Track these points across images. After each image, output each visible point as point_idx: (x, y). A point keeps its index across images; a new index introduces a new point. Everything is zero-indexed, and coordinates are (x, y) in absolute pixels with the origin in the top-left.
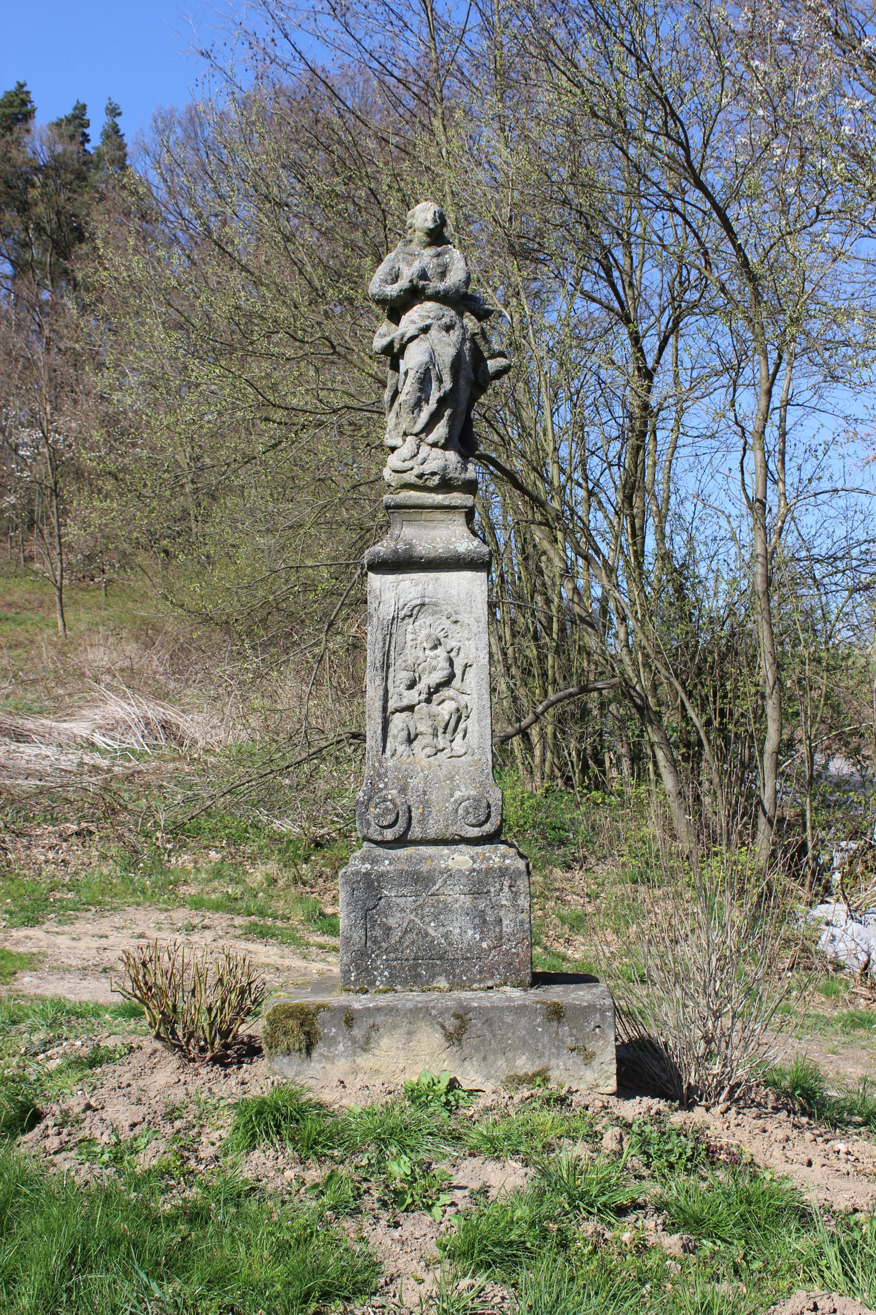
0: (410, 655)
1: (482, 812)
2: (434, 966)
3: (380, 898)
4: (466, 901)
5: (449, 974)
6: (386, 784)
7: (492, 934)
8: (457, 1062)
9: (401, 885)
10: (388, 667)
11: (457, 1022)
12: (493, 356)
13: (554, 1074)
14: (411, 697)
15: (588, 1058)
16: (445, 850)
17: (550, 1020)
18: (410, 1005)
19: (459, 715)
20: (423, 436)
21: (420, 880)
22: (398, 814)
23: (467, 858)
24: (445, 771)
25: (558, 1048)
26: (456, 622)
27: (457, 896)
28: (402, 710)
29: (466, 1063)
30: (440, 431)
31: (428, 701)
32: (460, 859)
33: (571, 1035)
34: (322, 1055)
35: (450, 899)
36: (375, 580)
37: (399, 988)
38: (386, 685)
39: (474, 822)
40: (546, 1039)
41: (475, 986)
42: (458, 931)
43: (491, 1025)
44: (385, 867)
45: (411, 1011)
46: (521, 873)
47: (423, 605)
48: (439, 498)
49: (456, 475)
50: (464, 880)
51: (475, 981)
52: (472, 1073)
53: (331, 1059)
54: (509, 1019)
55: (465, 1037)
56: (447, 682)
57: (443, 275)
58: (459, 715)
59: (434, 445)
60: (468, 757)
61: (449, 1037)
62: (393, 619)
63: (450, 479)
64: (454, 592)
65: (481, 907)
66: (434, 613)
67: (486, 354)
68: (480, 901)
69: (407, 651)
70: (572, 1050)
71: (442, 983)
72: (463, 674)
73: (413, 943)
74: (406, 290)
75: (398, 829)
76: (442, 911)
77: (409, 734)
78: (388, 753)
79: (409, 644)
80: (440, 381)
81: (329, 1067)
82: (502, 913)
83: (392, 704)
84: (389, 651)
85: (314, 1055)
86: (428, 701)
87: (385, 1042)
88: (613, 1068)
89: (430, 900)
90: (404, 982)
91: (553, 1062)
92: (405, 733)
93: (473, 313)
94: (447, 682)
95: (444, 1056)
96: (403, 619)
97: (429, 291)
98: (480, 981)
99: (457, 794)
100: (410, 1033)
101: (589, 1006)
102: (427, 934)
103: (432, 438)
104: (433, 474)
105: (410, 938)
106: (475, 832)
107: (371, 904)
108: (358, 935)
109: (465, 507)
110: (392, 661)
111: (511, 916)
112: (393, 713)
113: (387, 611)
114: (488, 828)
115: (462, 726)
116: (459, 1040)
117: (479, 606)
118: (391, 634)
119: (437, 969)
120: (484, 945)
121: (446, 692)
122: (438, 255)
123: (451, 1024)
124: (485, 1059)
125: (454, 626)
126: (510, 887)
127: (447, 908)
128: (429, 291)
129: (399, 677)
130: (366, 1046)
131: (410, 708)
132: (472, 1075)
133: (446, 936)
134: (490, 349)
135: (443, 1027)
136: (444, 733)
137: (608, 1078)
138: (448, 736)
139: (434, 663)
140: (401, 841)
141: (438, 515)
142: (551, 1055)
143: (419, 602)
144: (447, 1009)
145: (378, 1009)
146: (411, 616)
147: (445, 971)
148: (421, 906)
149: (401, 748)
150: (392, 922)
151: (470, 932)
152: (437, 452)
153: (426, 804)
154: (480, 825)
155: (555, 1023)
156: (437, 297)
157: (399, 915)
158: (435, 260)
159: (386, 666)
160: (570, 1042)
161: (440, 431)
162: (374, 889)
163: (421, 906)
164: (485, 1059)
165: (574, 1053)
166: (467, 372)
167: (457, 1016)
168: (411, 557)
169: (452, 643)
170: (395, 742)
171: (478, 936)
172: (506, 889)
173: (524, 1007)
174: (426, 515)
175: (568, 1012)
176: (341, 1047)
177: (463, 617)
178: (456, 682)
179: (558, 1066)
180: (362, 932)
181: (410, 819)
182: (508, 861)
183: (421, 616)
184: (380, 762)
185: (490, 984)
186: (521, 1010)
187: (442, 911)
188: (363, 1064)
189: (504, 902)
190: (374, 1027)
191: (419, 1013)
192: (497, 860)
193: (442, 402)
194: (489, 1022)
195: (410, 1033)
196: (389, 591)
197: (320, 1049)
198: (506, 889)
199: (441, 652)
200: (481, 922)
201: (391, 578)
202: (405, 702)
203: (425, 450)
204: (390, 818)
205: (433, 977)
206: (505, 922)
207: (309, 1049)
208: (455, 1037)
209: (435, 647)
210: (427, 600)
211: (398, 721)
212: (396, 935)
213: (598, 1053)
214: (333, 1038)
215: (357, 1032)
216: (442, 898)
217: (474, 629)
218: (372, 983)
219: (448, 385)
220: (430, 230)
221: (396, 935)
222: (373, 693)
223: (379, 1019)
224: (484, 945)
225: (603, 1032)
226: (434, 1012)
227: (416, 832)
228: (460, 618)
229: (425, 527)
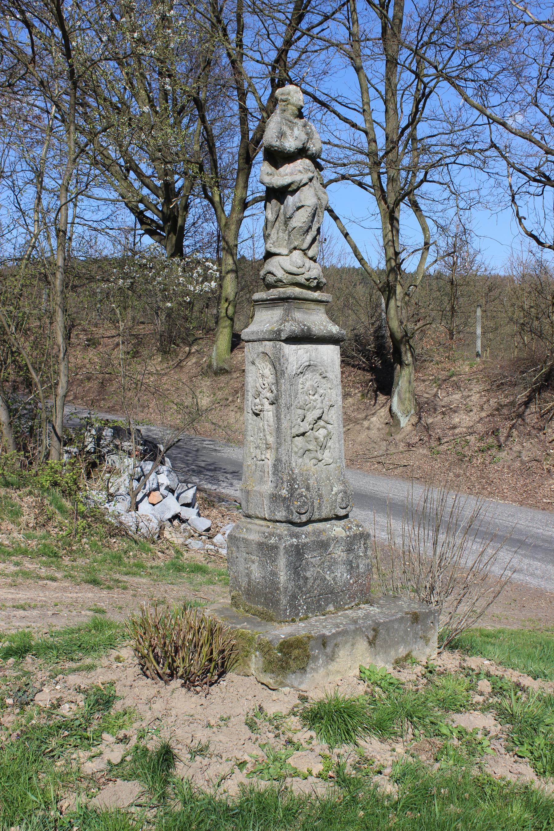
4: (344, 555)
5: (335, 602)
15: (427, 641)
21: (323, 546)
23: (341, 529)
26: (324, 378)
33: (422, 630)
34: (312, 668)
35: (337, 556)
41: (346, 607)
42: (340, 575)
44: (304, 539)
47: (309, 366)
51: (345, 604)
53: (315, 670)
64: (325, 358)
65: (351, 559)
66: (314, 371)
79: (300, 391)
81: (315, 675)
100: (353, 645)
102: (325, 579)
123: (371, 634)
125: (322, 380)
130: (332, 658)
139: (315, 404)
141: (312, 306)
143: (308, 364)
147: (333, 600)
148: (323, 563)
150: (308, 574)
153: (320, 496)
157: (312, 569)
163: (323, 563)
167: (374, 630)
168: (310, 335)
171: (349, 577)
176: (321, 661)
189: (361, 554)
190: (336, 645)
200: (351, 567)
201: (294, 347)
210: (312, 362)
215: (329, 650)
218: (297, 615)
223: (339, 639)
226: (364, 629)
228: (328, 375)
229: (307, 313)
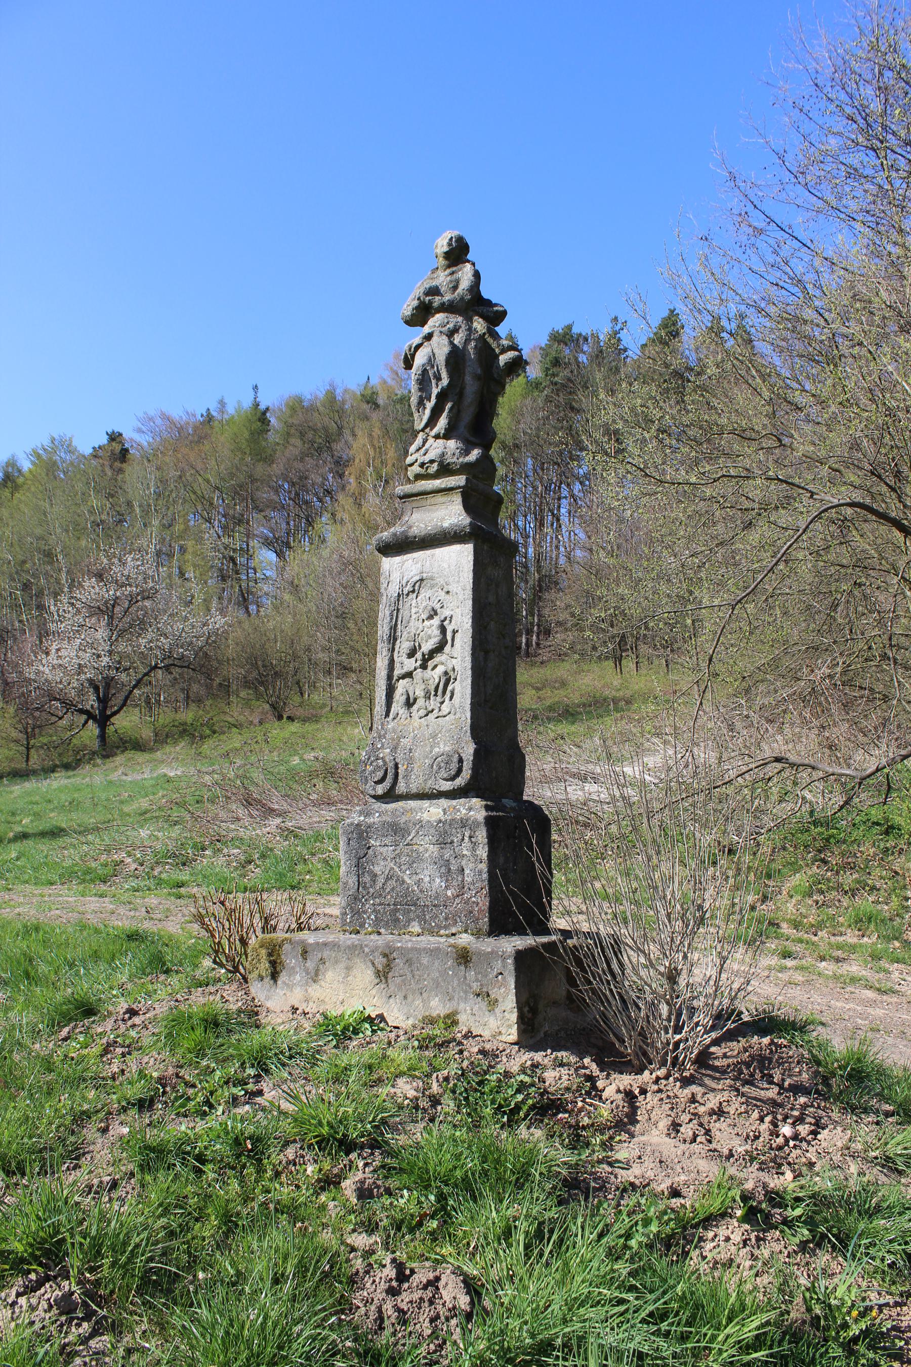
0: (414, 626)
1: (454, 766)
2: (409, 911)
3: (369, 848)
4: (433, 849)
5: (422, 919)
6: (383, 745)
7: (455, 883)
8: (384, 999)
9: (383, 836)
10: (395, 639)
11: (385, 960)
12: (503, 351)
13: (462, 1018)
14: (410, 664)
15: (493, 1004)
16: (426, 803)
17: (459, 964)
18: (349, 943)
19: (448, 679)
20: (427, 430)
21: (397, 830)
22: (386, 770)
23: (440, 810)
24: (430, 730)
25: (466, 992)
26: (448, 592)
27: (428, 847)
28: (403, 677)
29: (391, 1000)
30: (442, 423)
31: (424, 667)
32: (433, 811)
33: (477, 980)
34: (284, 982)
35: (421, 849)
36: (389, 564)
37: (382, 930)
38: (392, 656)
39: (445, 776)
40: (456, 982)
41: (442, 932)
42: (428, 879)
43: (410, 965)
44: (375, 819)
45: (349, 947)
46: (478, 824)
47: (422, 580)
48: (437, 483)
49: (455, 460)
50: (432, 831)
51: (440, 928)
52: (395, 1010)
53: (290, 987)
54: (425, 960)
55: (390, 975)
56: (439, 648)
57: (455, 288)
58: (448, 679)
59: (437, 437)
60: (451, 716)
61: (378, 973)
62: (399, 595)
63: (448, 464)
64: (445, 565)
65: (446, 856)
66: (432, 587)
67: (497, 351)
68: (445, 851)
69: (411, 624)
70: (478, 995)
71: (415, 928)
72: (453, 640)
73: (393, 889)
74: (416, 308)
75: (387, 784)
76: (415, 860)
77: (408, 698)
78: (391, 716)
79: (414, 616)
80: (438, 378)
81: (288, 994)
82: (464, 863)
83: (397, 672)
84: (396, 625)
85: (279, 982)
86: (424, 667)
87: (330, 975)
88: (514, 1017)
89: (407, 850)
90: (387, 926)
91: (462, 1006)
92: (405, 697)
93: (482, 316)
94: (439, 648)
95: (374, 992)
96: (408, 595)
97: (435, 305)
98: (446, 927)
99: (437, 750)
100: (348, 968)
101: (492, 953)
102: (403, 882)
103: (435, 431)
104: (432, 462)
105: (392, 883)
106: (447, 786)
107: (362, 854)
108: (352, 881)
109: (459, 487)
110: (399, 634)
111: (471, 865)
112: (398, 680)
113: (393, 590)
114: (460, 781)
115: (450, 688)
116: (386, 978)
117: (466, 575)
118: (398, 610)
119: (412, 915)
120: (449, 893)
121: (439, 658)
122: (453, 273)
123: (380, 961)
124: (405, 997)
125: (447, 597)
126: (470, 837)
127: (419, 859)
128: (435, 305)
129: (404, 646)
130: (315, 977)
131: (409, 675)
132: (396, 1013)
133: (419, 882)
134: (499, 345)
135: (373, 964)
136: (436, 695)
137: (510, 1026)
138: (439, 699)
139: (430, 632)
140: (390, 796)
141: (439, 498)
142: (460, 998)
143: (418, 578)
144: (377, 948)
145: (325, 944)
146: (413, 591)
147: (418, 917)
148: (399, 855)
149: (403, 711)
150: (377, 869)
151: (438, 880)
152: (441, 442)
153: (410, 761)
154: (453, 779)
155: (463, 968)
156: (443, 308)
157: (382, 863)
158: (449, 278)
159: (393, 639)
160: (476, 986)
161: (442, 423)
162: (364, 839)
163: (399, 855)
164: (405, 997)
165: (480, 999)
166: (472, 369)
167: (385, 955)
168: (407, 537)
169: (446, 613)
170: (398, 706)
171: (443, 884)
172: (466, 839)
173: (438, 949)
174: (431, 499)
175: (474, 958)
176: (298, 977)
177: (452, 588)
178: (447, 648)
179: (465, 1010)
180: (355, 878)
181: (396, 775)
182: (472, 813)
183: (422, 591)
184: (382, 724)
185: (454, 930)
186: (434, 952)
187: (415, 860)
188: (313, 993)
189: (465, 852)
190: (322, 961)
191: (354, 950)
192: (464, 812)
193: (442, 397)
194: (409, 962)
195: (348, 968)
196: (398, 570)
197: (283, 978)
198: (466, 839)
199: (436, 621)
200: (447, 871)
201: (397, 559)
202: (406, 669)
203: (431, 441)
204: (380, 774)
205: (409, 921)
206: (467, 871)
207: (274, 976)
208: (383, 975)
209: (431, 617)
210: (425, 575)
211: (401, 687)
212: (381, 880)
213: (500, 1000)
214: (293, 968)
215: (310, 964)
216: (415, 847)
217: (461, 597)
218: (362, 925)
219: (445, 381)
220: (446, 253)
221: (381, 880)
222: (381, 663)
223: (326, 954)
224: (449, 893)
225: (504, 979)
226: (366, 950)
227: (401, 788)
228: (450, 588)
229: (429, 511)
